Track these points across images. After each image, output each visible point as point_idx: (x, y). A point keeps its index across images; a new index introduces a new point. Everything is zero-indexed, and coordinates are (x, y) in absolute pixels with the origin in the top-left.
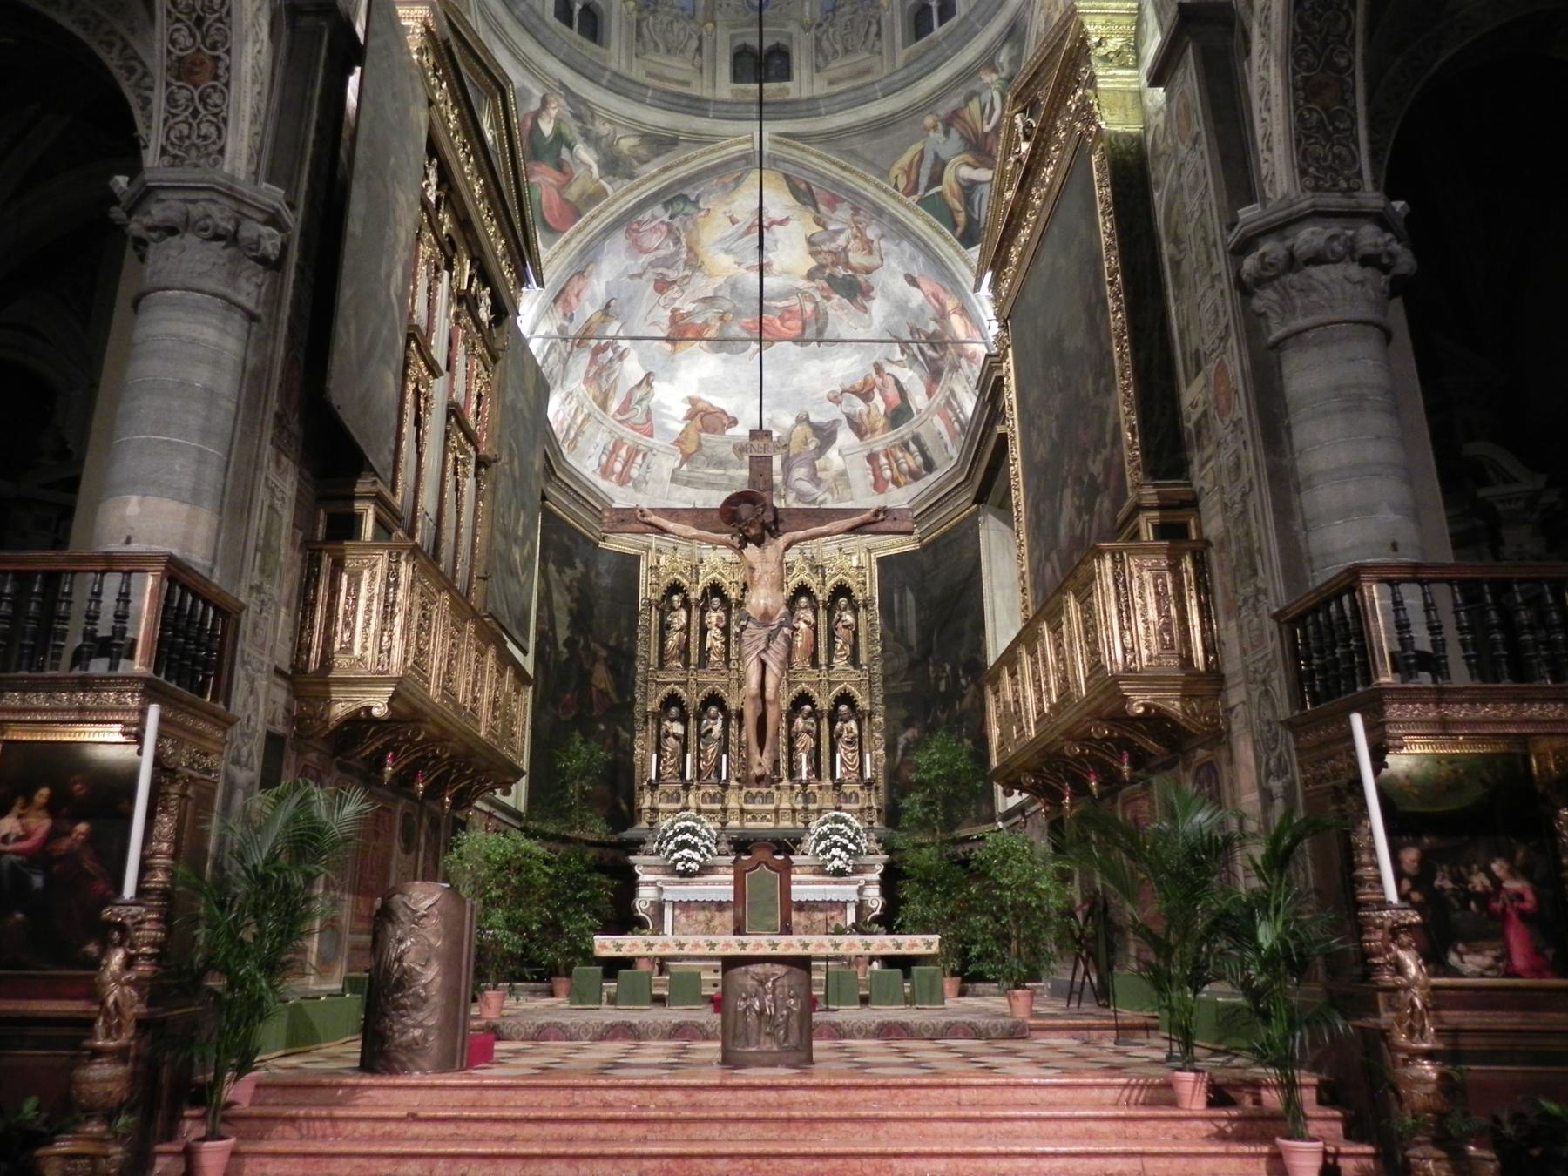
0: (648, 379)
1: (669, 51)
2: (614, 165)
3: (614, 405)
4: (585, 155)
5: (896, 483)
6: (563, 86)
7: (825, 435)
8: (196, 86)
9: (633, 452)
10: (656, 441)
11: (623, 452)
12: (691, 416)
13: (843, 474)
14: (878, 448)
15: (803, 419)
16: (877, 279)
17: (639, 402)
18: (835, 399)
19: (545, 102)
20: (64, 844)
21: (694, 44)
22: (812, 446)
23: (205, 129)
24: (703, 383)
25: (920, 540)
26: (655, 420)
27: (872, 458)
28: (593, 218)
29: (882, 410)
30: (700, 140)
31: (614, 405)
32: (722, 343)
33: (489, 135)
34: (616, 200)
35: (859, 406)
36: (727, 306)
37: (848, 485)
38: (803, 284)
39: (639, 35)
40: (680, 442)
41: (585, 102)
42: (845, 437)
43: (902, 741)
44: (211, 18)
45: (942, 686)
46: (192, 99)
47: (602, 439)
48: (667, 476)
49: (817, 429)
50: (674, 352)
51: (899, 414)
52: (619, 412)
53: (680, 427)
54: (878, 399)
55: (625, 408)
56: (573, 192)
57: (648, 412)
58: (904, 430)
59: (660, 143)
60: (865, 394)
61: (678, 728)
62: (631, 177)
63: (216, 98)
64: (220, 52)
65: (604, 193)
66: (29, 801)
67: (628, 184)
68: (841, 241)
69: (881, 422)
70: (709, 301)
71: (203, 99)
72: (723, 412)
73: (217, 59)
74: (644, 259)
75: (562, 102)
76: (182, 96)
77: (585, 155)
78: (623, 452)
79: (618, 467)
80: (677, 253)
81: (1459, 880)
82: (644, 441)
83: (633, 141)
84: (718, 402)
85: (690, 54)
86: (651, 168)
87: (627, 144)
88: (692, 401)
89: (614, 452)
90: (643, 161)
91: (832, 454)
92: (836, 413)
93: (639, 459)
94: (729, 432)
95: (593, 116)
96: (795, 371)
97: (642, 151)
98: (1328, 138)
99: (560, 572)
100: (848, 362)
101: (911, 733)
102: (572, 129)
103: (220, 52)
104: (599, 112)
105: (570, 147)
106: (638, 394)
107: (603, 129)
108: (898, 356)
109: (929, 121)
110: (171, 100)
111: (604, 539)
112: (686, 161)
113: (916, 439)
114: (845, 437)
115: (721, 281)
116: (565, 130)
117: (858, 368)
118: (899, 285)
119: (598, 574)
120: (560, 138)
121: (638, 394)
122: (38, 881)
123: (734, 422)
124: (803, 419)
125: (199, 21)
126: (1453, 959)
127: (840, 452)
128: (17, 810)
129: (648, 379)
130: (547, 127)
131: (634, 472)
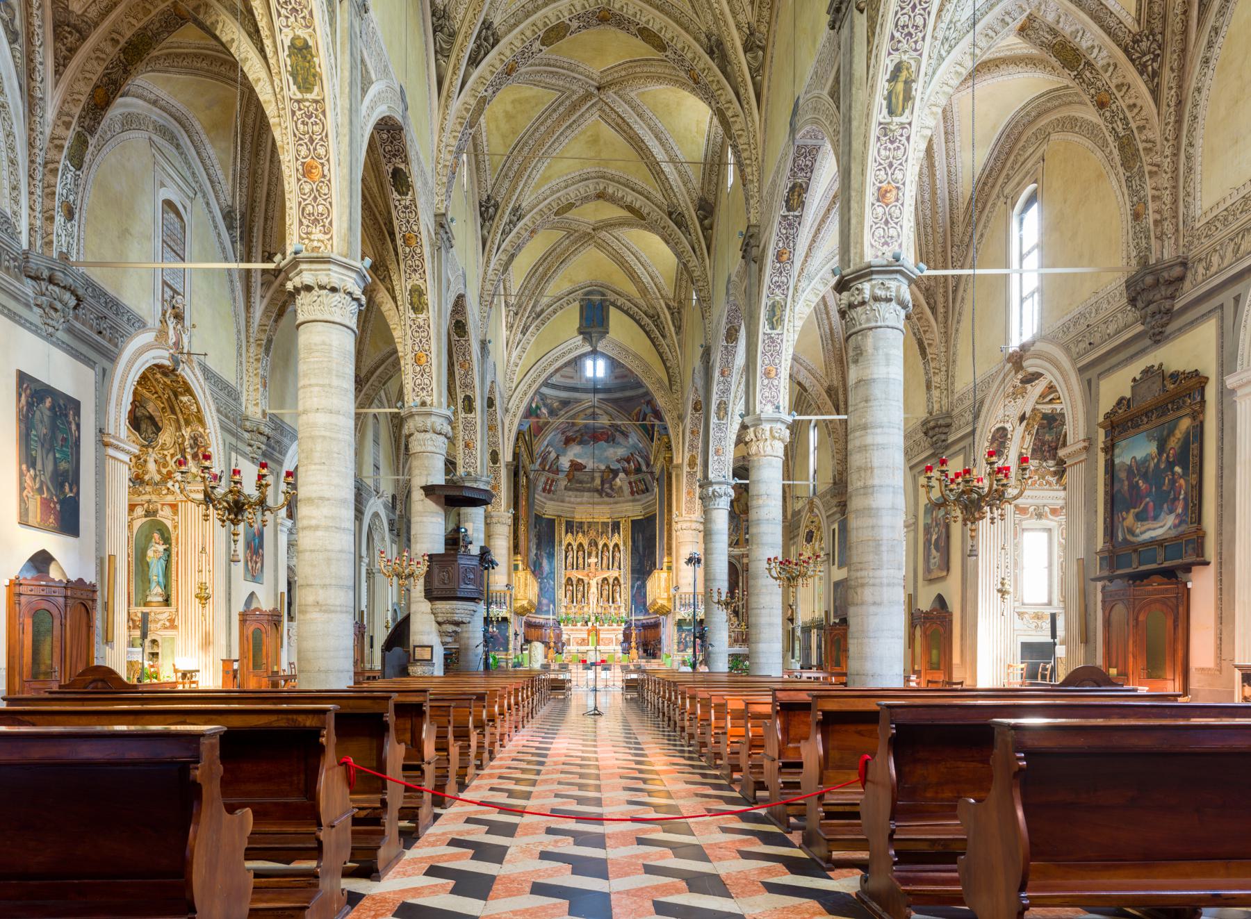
0: (557, 457)
2: (552, 412)
7: (615, 473)
13: (621, 487)
15: (608, 467)
18: (618, 461)
24: (575, 455)
27: (630, 483)
32: (581, 443)
35: (626, 465)
42: (622, 475)
49: (612, 471)
51: (638, 470)
58: (640, 476)
60: (628, 461)
70: (577, 431)
77: (544, 411)
84: (579, 461)
87: (556, 405)
92: (618, 466)
102: (541, 404)
107: (549, 401)
114: (622, 475)
120: (538, 407)
124: (608, 467)
129: (557, 457)
130: (534, 405)
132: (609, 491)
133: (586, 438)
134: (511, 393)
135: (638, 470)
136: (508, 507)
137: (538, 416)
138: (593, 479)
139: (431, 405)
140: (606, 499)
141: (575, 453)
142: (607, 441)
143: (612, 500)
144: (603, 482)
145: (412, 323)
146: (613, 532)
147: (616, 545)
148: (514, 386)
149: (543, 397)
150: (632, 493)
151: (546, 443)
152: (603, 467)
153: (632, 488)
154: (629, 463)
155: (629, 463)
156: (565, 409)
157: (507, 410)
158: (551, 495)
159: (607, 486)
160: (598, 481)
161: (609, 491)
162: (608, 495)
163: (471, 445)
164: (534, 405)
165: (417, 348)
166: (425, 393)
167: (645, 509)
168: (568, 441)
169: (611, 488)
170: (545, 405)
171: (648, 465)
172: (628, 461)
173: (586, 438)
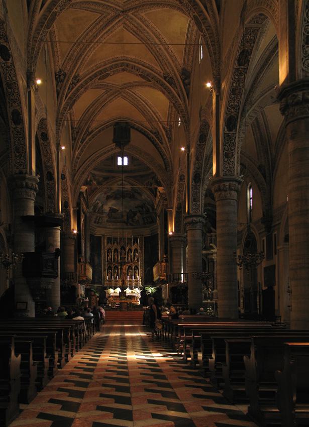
2: (99, 183)
7: (135, 214)
10: (104, 215)
12: (110, 210)
15: (131, 210)
27: (143, 218)
31: (97, 211)
32: (116, 198)
33: (85, 196)
35: (141, 209)
41: (94, 174)
42: (138, 214)
48: (106, 221)
54: (144, 209)
56: (93, 188)
77: (95, 182)
88: (110, 208)
89: (96, 219)
91: (136, 217)
101: (149, 268)
105: (92, 181)
107: (97, 178)
114: (138, 214)
129: (102, 206)
130: (89, 180)
131: (100, 221)
132: (131, 222)
134: (75, 172)
138: (123, 216)
139: (26, 173)
140: (130, 226)
144: (128, 219)
145: (13, 130)
146: (134, 243)
147: (136, 250)
148: (77, 169)
149: (94, 175)
151: (96, 198)
152: (128, 211)
154: (142, 208)
159: (130, 220)
161: (131, 222)
162: (131, 224)
164: (89, 180)
165: (17, 144)
166: (22, 167)
167: (151, 231)
170: (95, 180)
171: (153, 209)
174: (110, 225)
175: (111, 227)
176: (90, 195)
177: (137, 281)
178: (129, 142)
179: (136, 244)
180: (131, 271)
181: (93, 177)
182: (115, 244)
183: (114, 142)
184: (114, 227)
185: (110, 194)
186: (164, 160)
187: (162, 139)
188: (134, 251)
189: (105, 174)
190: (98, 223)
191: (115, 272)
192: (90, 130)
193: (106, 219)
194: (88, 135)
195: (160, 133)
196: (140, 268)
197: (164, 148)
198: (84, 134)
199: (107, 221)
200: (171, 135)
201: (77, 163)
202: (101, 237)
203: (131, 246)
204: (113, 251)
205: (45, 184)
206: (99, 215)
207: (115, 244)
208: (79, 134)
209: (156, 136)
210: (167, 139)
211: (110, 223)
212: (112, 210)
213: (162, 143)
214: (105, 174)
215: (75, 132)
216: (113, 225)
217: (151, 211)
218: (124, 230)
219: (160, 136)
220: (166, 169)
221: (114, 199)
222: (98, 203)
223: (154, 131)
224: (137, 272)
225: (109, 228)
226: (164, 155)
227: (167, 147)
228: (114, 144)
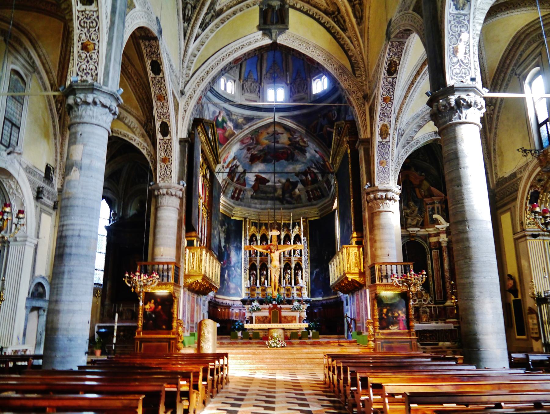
0: (244, 172)
1: (251, 92)
2: (237, 126)
3: (235, 179)
4: (230, 124)
5: (315, 200)
6: (224, 108)
7: (295, 185)
8: (88, 52)
9: (240, 191)
11: (238, 191)
12: (256, 180)
13: (299, 196)
14: (309, 189)
15: (288, 180)
16: (308, 149)
17: (242, 177)
19: (220, 113)
20: (158, 310)
21: (258, 89)
22: (290, 188)
23: (168, 172)
25: (320, 216)
26: (246, 182)
27: (307, 192)
28: (232, 140)
29: (310, 179)
30: (260, 118)
31: (235, 179)
34: (237, 135)
35: (304, 178)
36: (266, 151)
37: (301, 199)
38: (287, 146)
39: (243, 88)
40: (253, 187)
41: (230, 111)
42: (300, 186)
43: (315, 272)
44: (168, 150)
45: (326, 257)
46: (87, 56)
47: (232, 189)
48: (249, 196)
50: (252, 164)
52: (237, 181)
53: (253, 183)
54: (309, 176)
55: (238, 179)
56: (227, 134)
57: (244, 180)
58: (316, 185)
59: (249, 119)
61: (255, 272)
62: (242, 129)
63: (169, 166)
64: (170, 157)
65: (234, 134)
66: (150, 302)
67: (241, 131)
68: (297, 139)
69: (310, 183)
70: (261, 151)
71: (167, 166)
72: (265, 179)
73: (169, 158)
74: (244, 145)
75: (224, 112)
76: (163, 166)
77: (230, 124)
78: (238, 191)
79: (236, 195)
80: (253, 142)
81: (393, 314)
82: (243, 188)
83: (242, 120)
84: (263, 176)
85: (257, 92)
86: (247, 127)
87: (240, 120)
89: (234, 192)
90: (245, 125)
91: (297, 190)
92: (297, 179)
93: (242, 193)
94: (267, 184)
95: (232, 114)
96: (286, 167)
97: (244, 122)
98: (384, 173)
99: (222, 227)
100: (300, 166)
101: (317, 270)
102: (226, 118)
103: (170, 157)
104: (233, 113)
105: (226, 123)
106: (242, 176)
107: (234, 117)
108: (314, 166)
109: (319, 115)
110: (161, 167)
111: (233, 216)
112: (256, 124)
113: (319, 188)
114: (300, 186)
115: (264, 146)
116: (225, 119)
117: (303, 168)
118: (313, 152)
119: (231, 226)
120: (224, 121)
121: (242, 176)
122: (154, 316)
123: (268, 181)
125: (166, 151)
126: (390, 327)
127: (299, 190)
128: (149, 304)
129: (244, 172)
130: (220, 119)
131: (241, 197)
132: (289, 199)
133: (269, 157)
134: (188, 79)
135: (315, 180)
136: (180, 179)
137: (224, 129)
140: (286, 206)
141: (259, 167)
142: (287, 160)
143: (292, 206)
144: (284, 193)
145: (80, 15)
146: (294, 226)
150: (309, 200)
152: (284, 181)
153: (309, 195)
154: (306, 176)
155: (306, 176)
156: (250, 124)
157: (182, 93)
158: (239, 202)
159: (287, 195)
160: (279, 192)
161: (289, 199)
162: (289, 203)
163: (91, 47)
164: (220, 119)
167: (320, 211)
168: (253, 159)
169: (291, 196)
172: (305, 173)
173: (269, 157)
174: (256, 204)
175: (258, 206)
176: (221, 144)
177: (300, 290)
178: (288, 29)
179: (297, 227)
180: (289, 271)
181: (228, 115)
182: (264, 228)
183: (260, 28)
184: (263, 206)
185: (256, 152)
186: (349, 58)
187: (344, 21)
188: (295, 238)
189: (248, 113)
190: (237, 199)
191: (261, 274)
192: (218, 8)
193: (249, 194)
194: (212, 16)
195: (343, 9)
196: (303, 266)
197: (349, 38)
198: (207, 14)
199: (252, 197)
200: (362, 11)
201: (192, 63)
202: (242, 221)
203: (290, 230)
204: (259, 238)
205: (75, 14)
206: (239, 186)
207: (264, 228)
208: (197, 10)
209: (333, 19)
210: (354, 20)
211: (256, 201)
212: (260, 180)
213: (344, 30)
214: (248, 113)
215: (189, 6)
216: (261, 204)
217: (320, 178)
218: (276, 211)
219: (342, 17)
220: (354, 71)
221: (263, 162)
222: (237, 167)
223: (331, 9)
224: (300, 273)
225: (255, 208)
226: (349, 50)
227: (355, 34)
228: (261, 32)
